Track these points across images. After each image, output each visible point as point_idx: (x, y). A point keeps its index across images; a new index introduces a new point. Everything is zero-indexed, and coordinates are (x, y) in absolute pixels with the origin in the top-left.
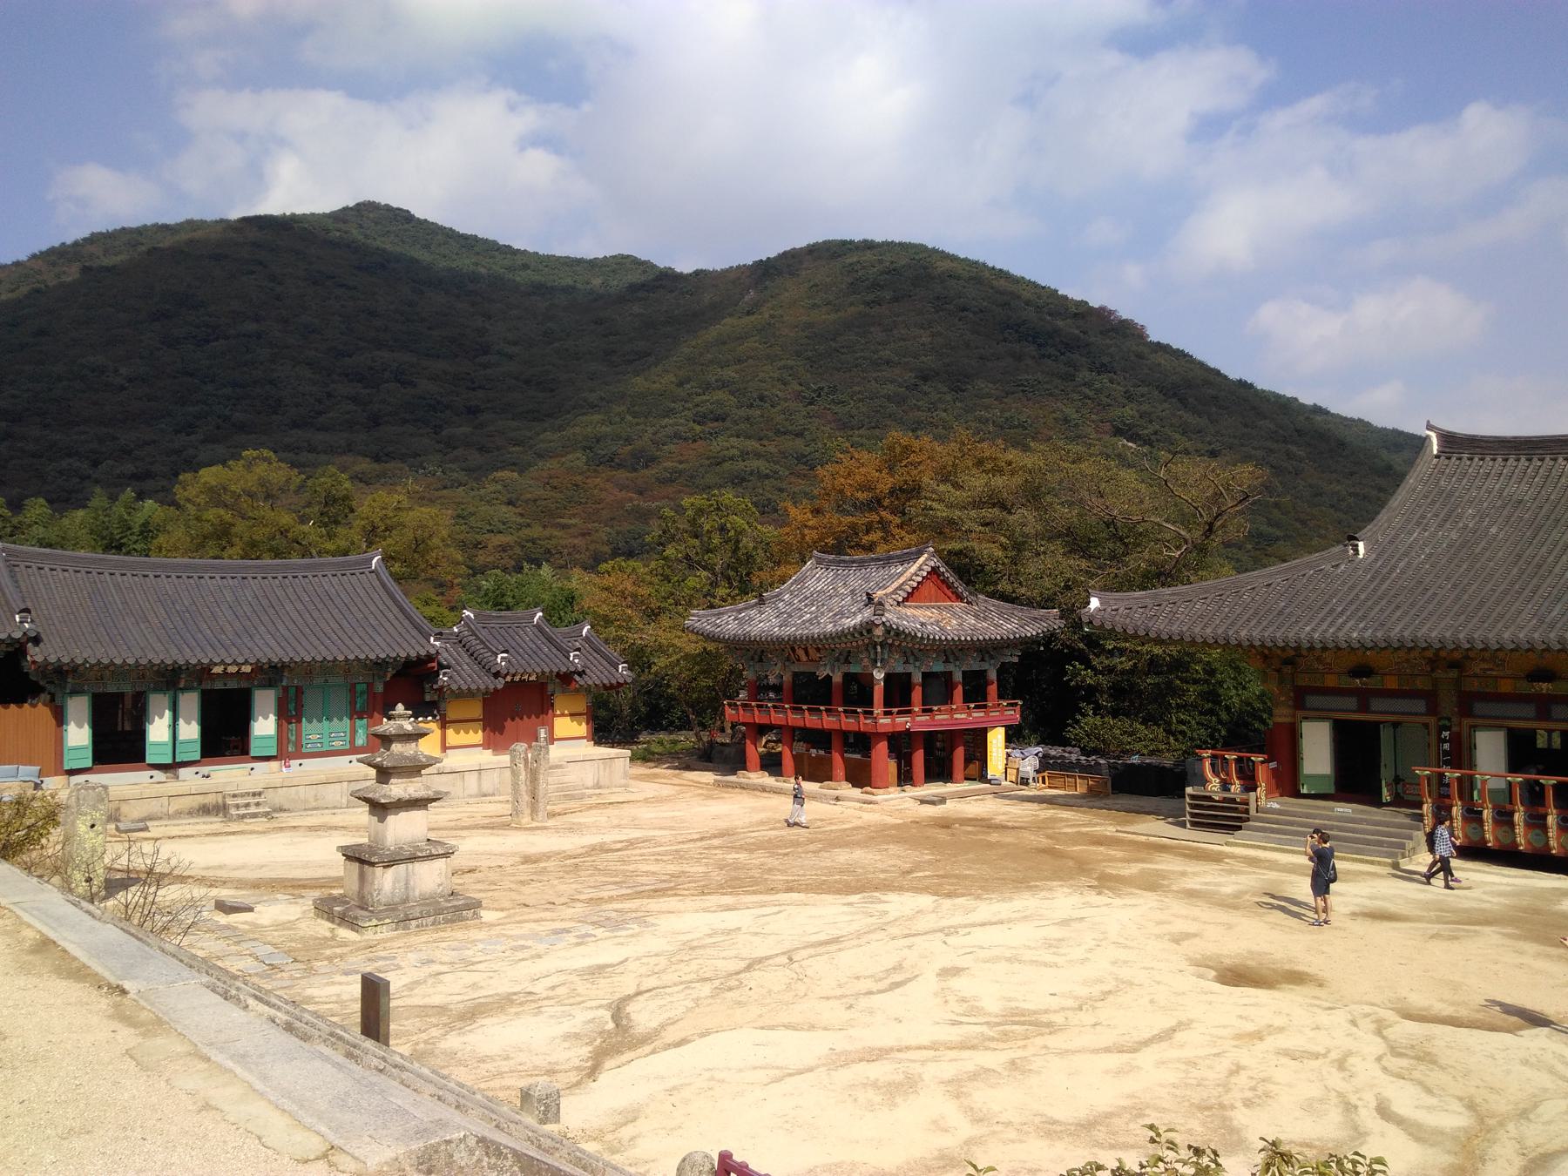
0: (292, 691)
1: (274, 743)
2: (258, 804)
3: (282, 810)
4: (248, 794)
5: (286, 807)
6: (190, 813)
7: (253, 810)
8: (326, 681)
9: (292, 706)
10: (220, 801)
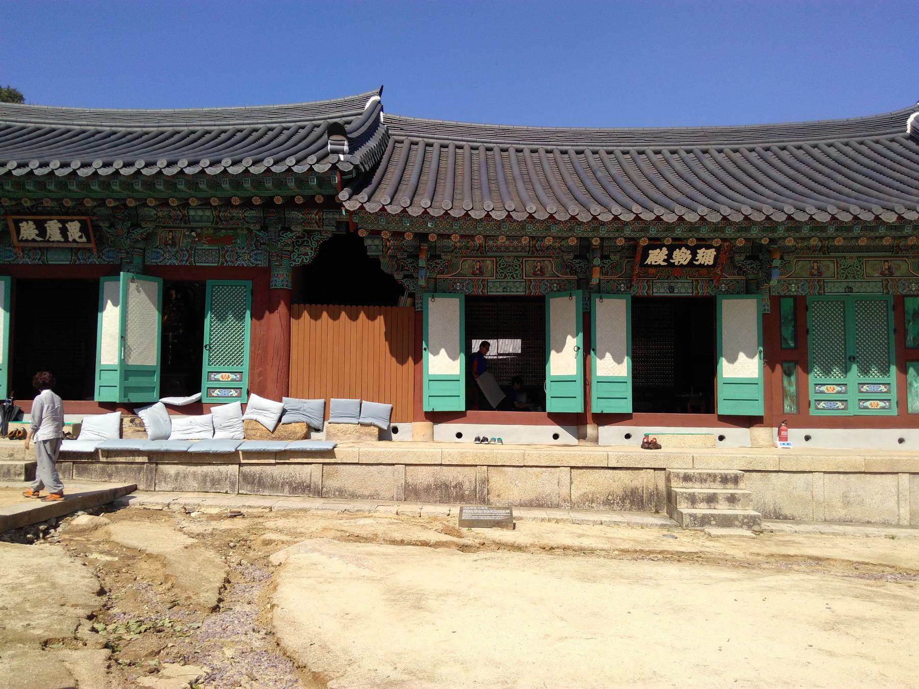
0: (787, 306)
1: (758, 393)
2: (732, 499)
3: (778, 516)
4: (713, 477)
5: (786, 511)
6: (609, 503)
7: (723, 509)
8: (850, 289)
9: (787, 332)
10: (662, 486)
